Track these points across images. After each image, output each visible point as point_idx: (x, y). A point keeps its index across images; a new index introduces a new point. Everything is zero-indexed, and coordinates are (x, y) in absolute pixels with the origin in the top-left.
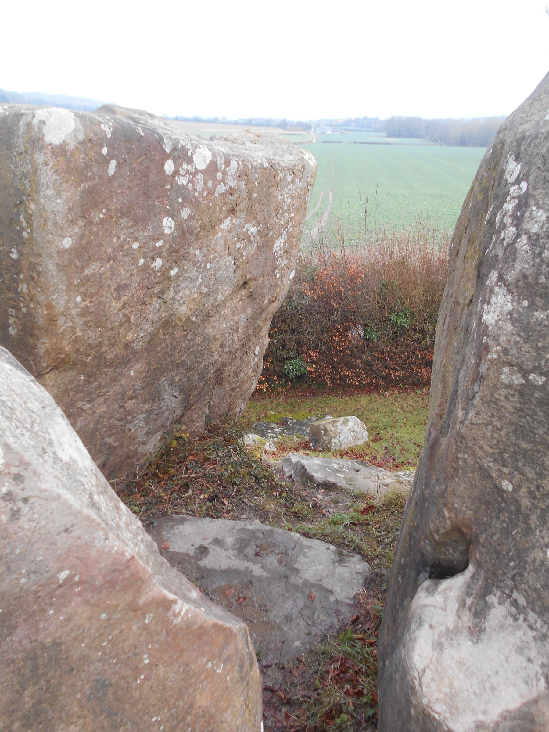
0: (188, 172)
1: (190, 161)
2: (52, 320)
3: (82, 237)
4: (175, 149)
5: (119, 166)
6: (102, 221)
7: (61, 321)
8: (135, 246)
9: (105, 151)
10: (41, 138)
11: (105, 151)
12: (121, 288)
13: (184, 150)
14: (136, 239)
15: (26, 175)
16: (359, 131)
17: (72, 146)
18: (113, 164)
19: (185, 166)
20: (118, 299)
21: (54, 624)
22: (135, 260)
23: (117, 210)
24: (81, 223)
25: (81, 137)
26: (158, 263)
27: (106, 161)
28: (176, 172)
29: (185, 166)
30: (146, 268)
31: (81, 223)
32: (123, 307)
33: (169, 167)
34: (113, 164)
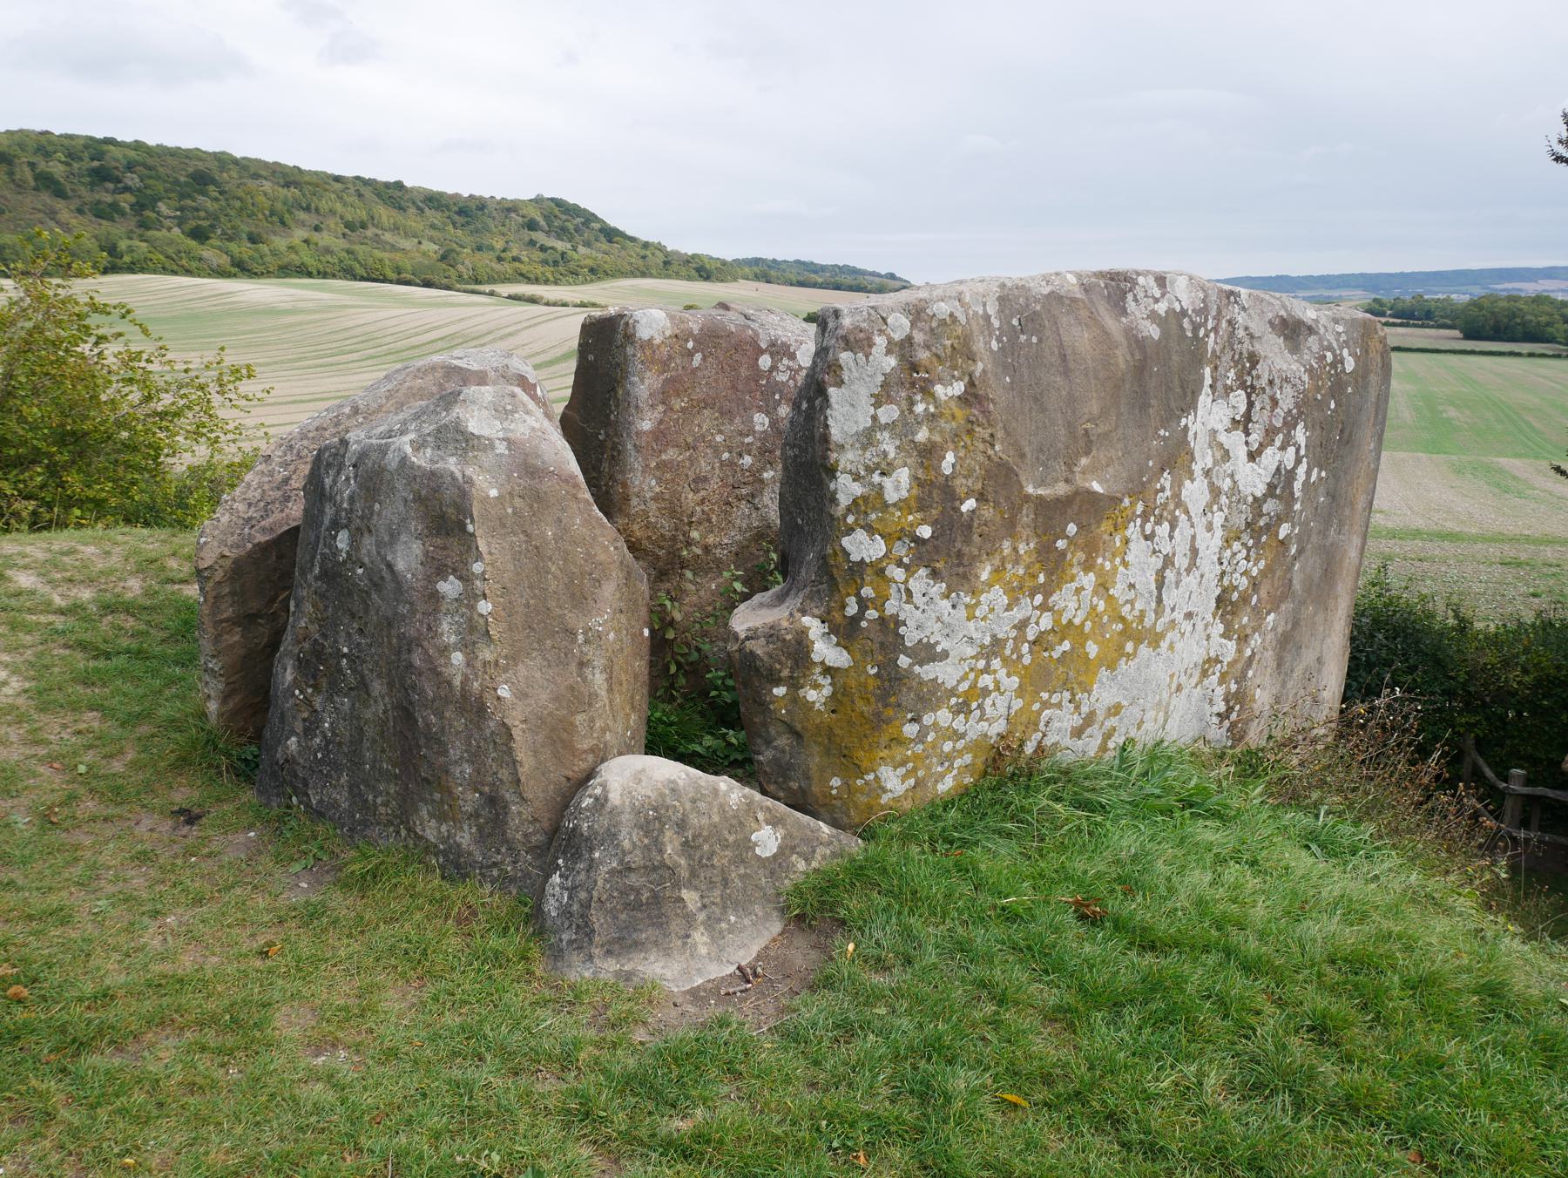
0: (788, 368)
1: (792, 357)
2: (627, 499)
3: (661, 422)
4: (773, 344)
5: (704, 359)
6: (683, 410)
7: (634, 501)
8: (719, 438)
9: (690, 345)
10: (634, 335)
11: (690, 345)
12: (701, 480)
13: (786, 346)
14: (720, 432)
15: (618, 365)
16: (1401, 325)
17: (657, 341)
18: (698, 357)
19: (785, 361)
20: (696, 491)
21: (547, 485)
22: (717, 451)
23: (699, 401)
24: (661, 408)
25: (668, 333)
26: (747, 460)
27: (691, 354)
28: (774, 368)
29: (785, 361)
30: (731, 464)
31: (661, 408)
32: (703, 502)
33: (765, 362)
34: (698, 357)
